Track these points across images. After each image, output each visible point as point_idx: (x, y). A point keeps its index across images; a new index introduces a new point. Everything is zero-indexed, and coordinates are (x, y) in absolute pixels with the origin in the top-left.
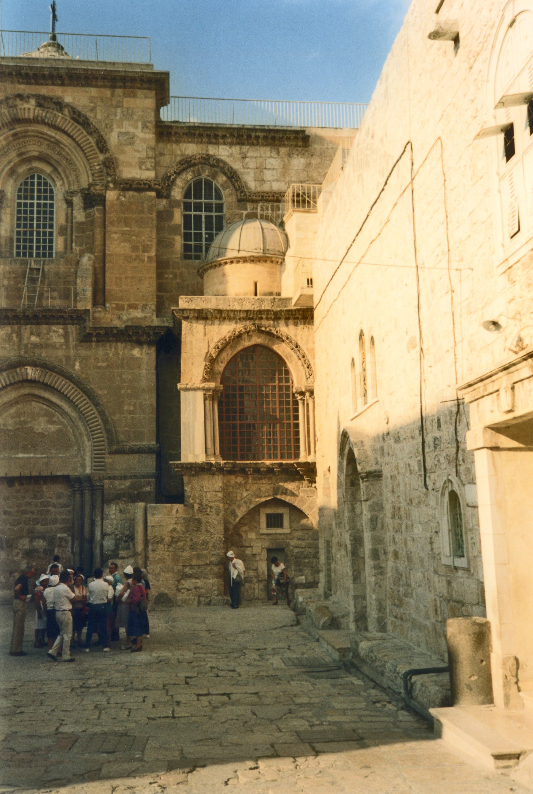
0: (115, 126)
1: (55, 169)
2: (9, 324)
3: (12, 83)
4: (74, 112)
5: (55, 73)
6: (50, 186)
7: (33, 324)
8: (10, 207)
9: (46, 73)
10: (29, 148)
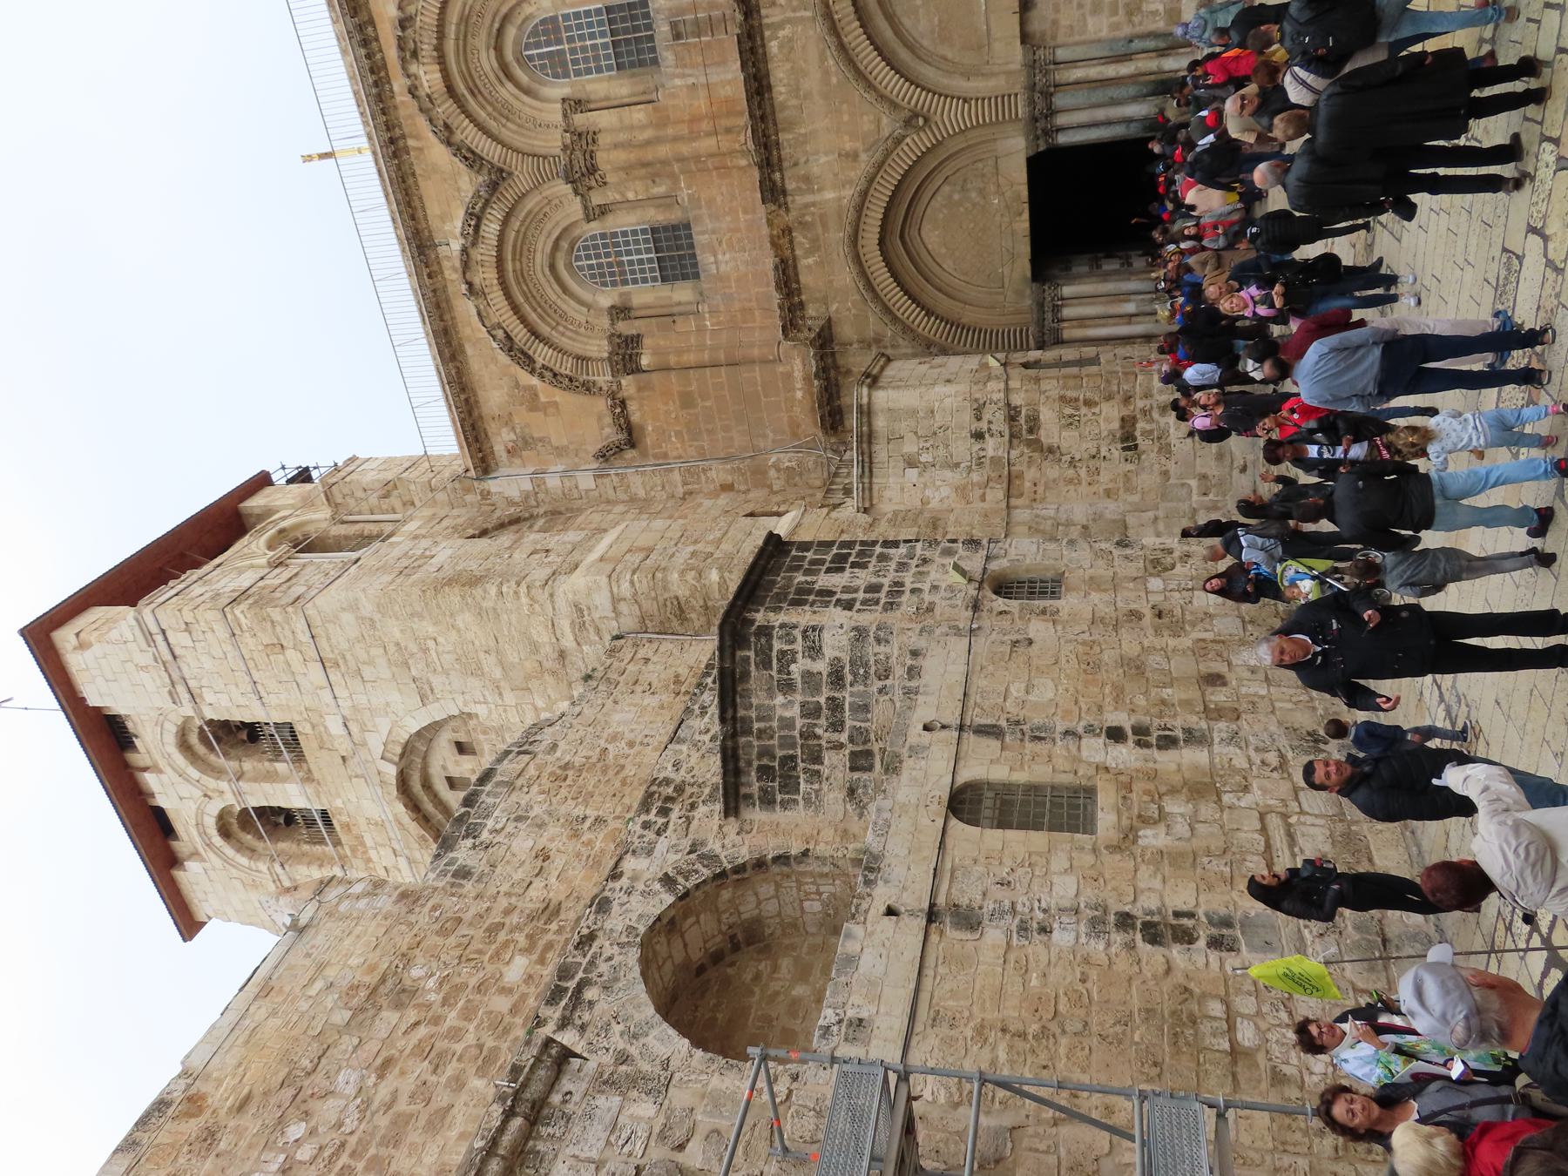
1: (506, 19)
2: (763, 46)
3: (395, 107)
6: (536, 25)
8: (584, 86)
10: (487, 68)
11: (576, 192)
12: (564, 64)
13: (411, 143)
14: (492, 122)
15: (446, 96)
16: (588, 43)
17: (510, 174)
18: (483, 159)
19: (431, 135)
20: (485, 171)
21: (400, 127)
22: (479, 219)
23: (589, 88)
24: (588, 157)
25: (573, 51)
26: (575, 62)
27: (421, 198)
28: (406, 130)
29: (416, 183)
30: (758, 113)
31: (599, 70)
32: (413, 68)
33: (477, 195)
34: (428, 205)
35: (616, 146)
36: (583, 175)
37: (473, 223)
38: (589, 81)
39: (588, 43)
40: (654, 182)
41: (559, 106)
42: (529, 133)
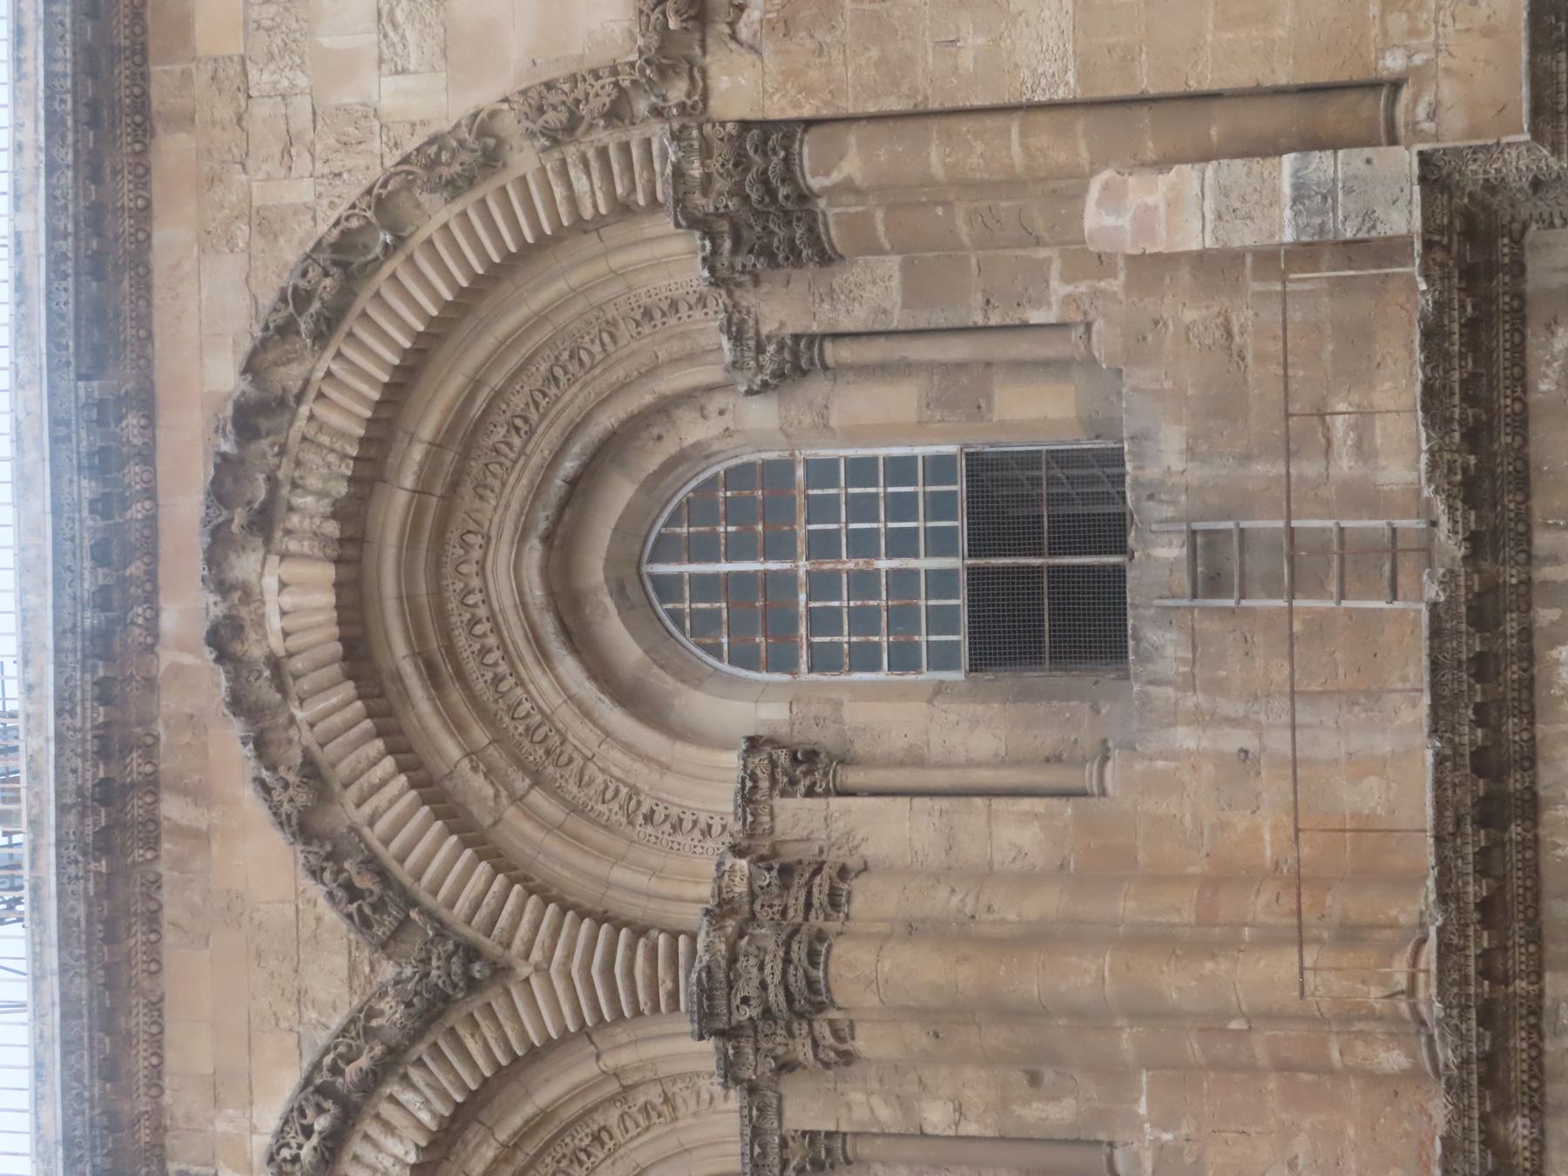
0: (348, 98)
2: (1528, 656)
3: (150, 684)
4: (286, 330)
5: (84, 439)
6: (711, 483)
7: (1524, 516)
8: (838, 705)
9: (87, 488)
11: (730, 1072)
12: (780, 624)
13: (173, 809)
14: (479, 782)
15: (335, 670)
16: (883, 564)
17: (500, 970)
18: (412, 902)
19: (248, 794)
20: (413, 945)
21: (150, 750)
22: (349, 1116)
23: (856, 714)
24: (799, 951)
25: (822, 584)
26: (823, 621)
27: (156, 1006)
28: (168, 764)
29: (154, 953)
30: (1473, 890)
31: (904, 659)
32: (246, 565)
33: (361, 1025)
34: (175, 1031)
35: (911, 930)
36: (767, 1013)
37: (321, 1124)
38: (859, 691)
39: (883, 564)
40: (1034, 1079)
41: (732, 760)
42: (599, 837)
